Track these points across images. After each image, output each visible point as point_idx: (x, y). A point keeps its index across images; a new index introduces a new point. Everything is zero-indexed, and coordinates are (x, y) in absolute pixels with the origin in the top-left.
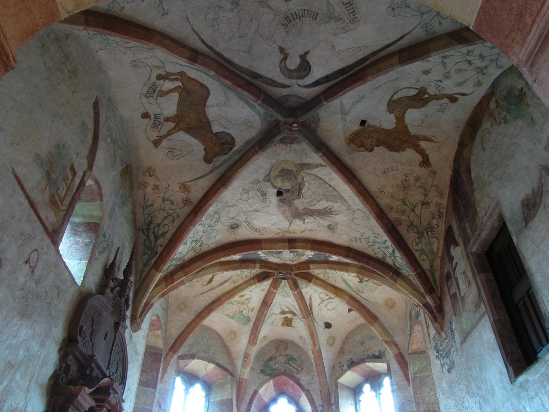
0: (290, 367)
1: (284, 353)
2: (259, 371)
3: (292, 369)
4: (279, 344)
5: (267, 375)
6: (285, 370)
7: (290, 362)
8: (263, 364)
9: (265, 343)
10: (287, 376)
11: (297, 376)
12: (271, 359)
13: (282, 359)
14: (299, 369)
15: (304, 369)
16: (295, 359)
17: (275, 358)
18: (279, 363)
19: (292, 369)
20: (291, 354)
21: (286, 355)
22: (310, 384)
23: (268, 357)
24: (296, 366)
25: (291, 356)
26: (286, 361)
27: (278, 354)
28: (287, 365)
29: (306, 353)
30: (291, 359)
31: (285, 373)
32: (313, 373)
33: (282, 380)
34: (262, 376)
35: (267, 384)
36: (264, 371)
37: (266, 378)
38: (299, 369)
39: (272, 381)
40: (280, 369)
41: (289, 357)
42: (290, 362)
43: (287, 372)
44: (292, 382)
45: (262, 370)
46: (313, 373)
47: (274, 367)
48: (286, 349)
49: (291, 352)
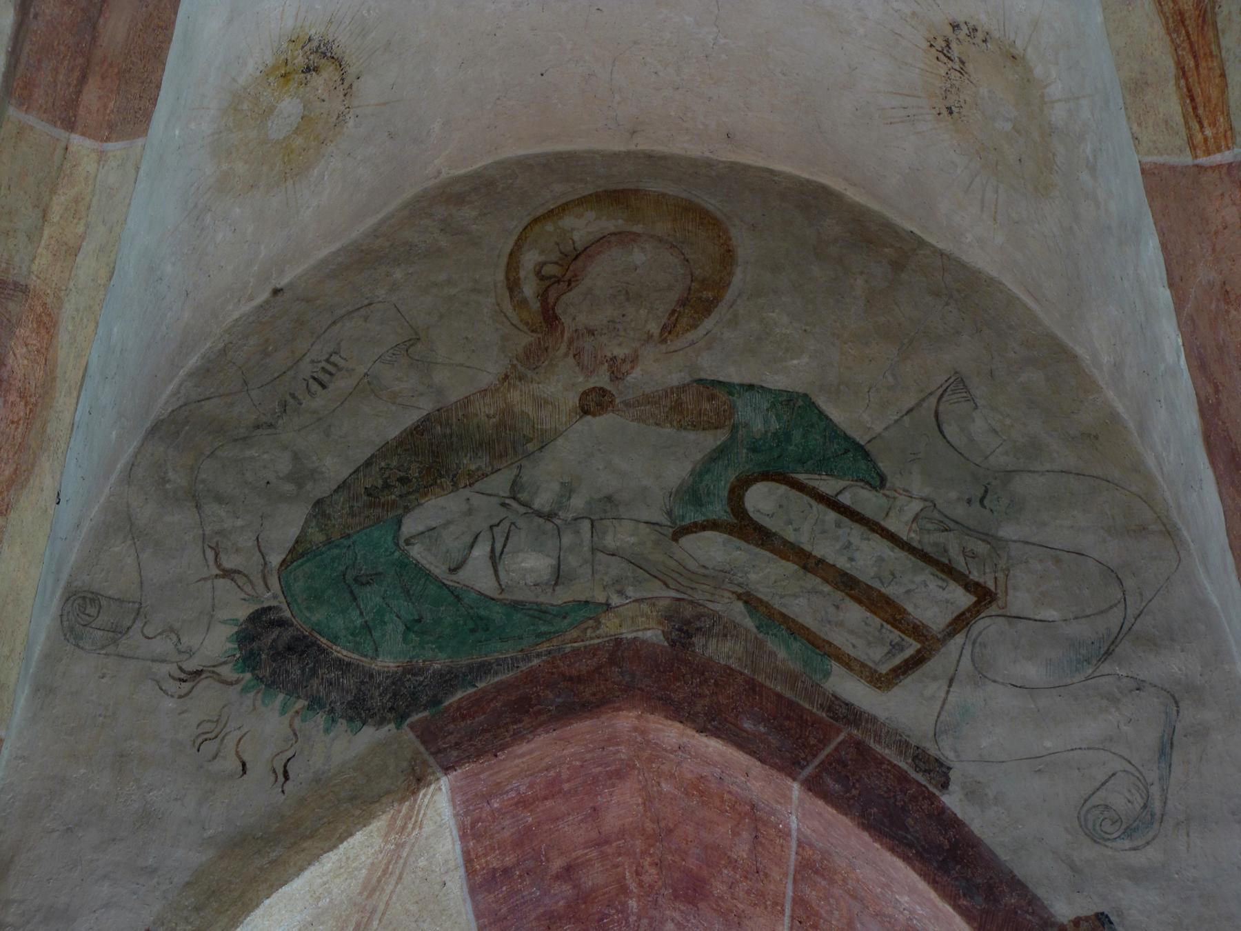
0: (767, 574)
1: (658, 371)
2: (216, 643)
3: (807, 603)
4: (582, 227)
5: (359, 711)
6: (685, 628)
7: (762, 500)
8: (288, 525)
9: (326, 208)
10: (714, 722)
11: (904, 709)
12: (430, 456)
13: (647, 465)
14: (934, 602)
15: (1020, 600)
16: (857, 457)
17: (509, 442)
18: (593, 511)
19: (807, 603)
20: (791, 375)
21: (702, 403)
22: (1141, 824)
23: (383, 425)
24: (866, 557)
25: (798, 406)
26: (692, 493)
27: (561, 385)
28: (712, 549)
29: (1057, 357)
30: (802, 446)
31: (677, 675)
32: (1173, 665)
33: (622, 805)
34: (266, 723)
35: (363, 846)
36: (302, 647)
37: (344, 747)
38: (934, 602)
39: (439, 803)
40: (595, 610)
41: (756, 420)
42: (762, 500)
43: (720, 651)
44: (798, 812)
45: (260, 624)
46: (1173, 665)
47: (477, 575)
48: (698, 301)
49: (777, 347)
